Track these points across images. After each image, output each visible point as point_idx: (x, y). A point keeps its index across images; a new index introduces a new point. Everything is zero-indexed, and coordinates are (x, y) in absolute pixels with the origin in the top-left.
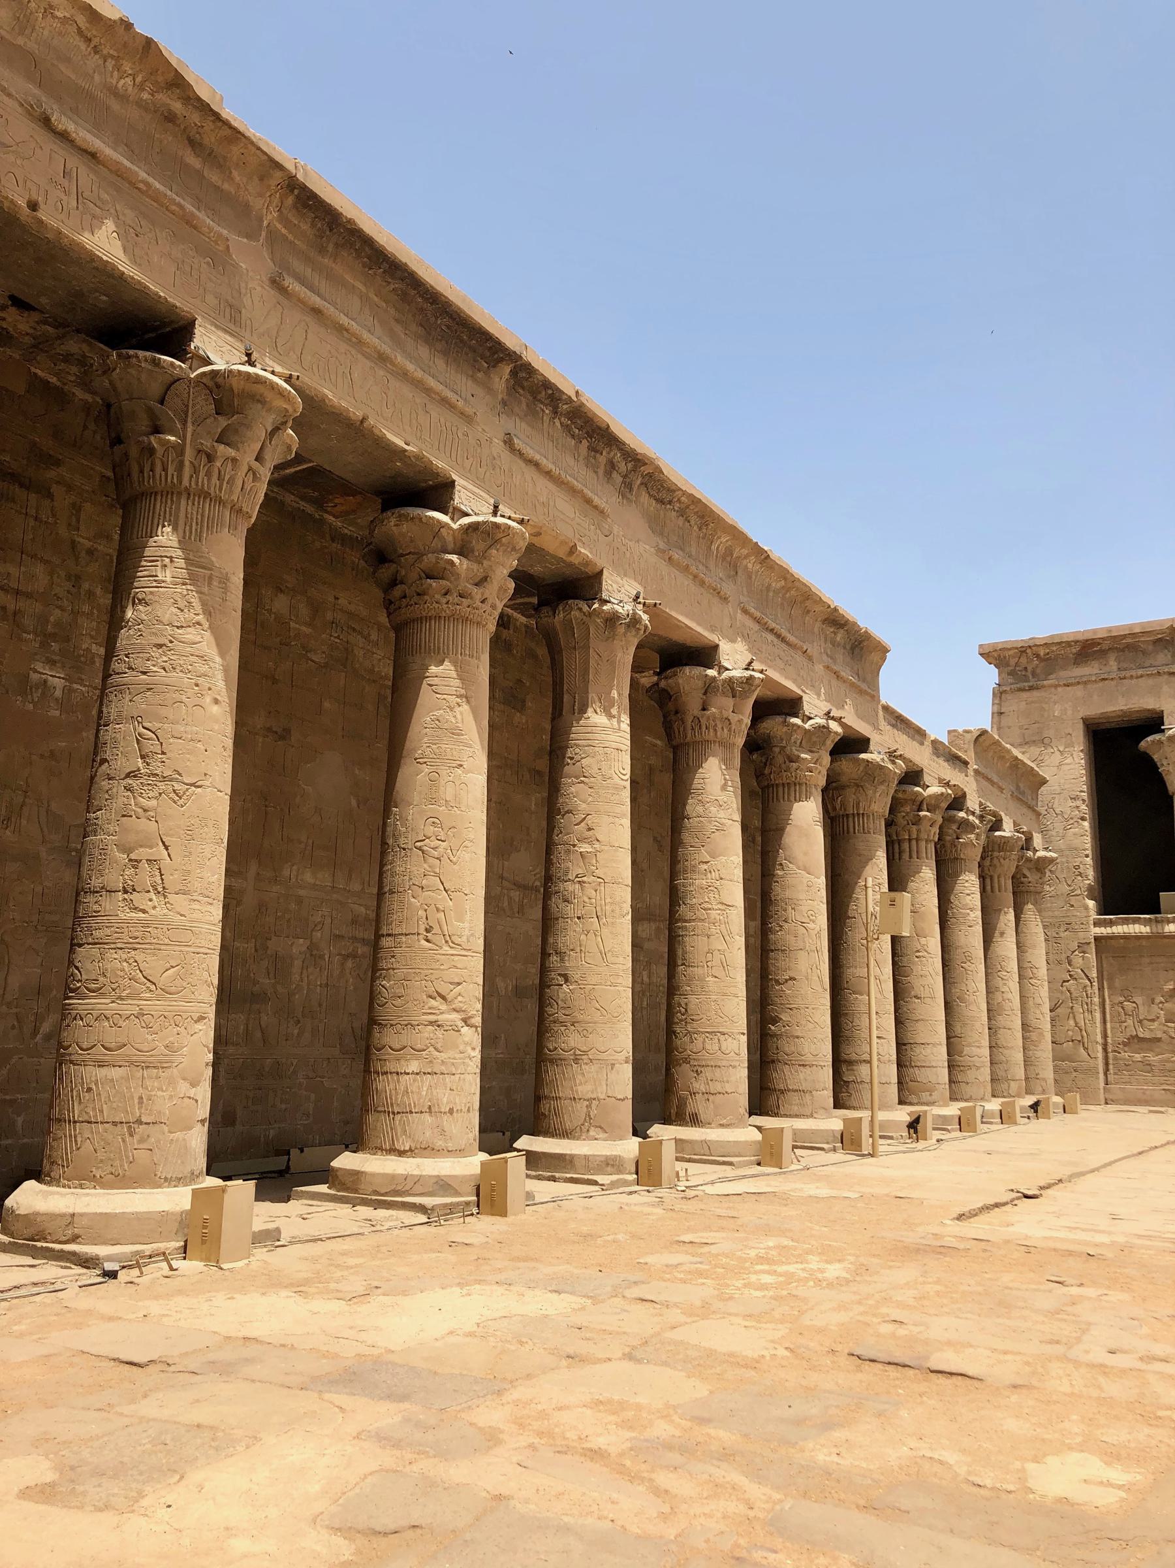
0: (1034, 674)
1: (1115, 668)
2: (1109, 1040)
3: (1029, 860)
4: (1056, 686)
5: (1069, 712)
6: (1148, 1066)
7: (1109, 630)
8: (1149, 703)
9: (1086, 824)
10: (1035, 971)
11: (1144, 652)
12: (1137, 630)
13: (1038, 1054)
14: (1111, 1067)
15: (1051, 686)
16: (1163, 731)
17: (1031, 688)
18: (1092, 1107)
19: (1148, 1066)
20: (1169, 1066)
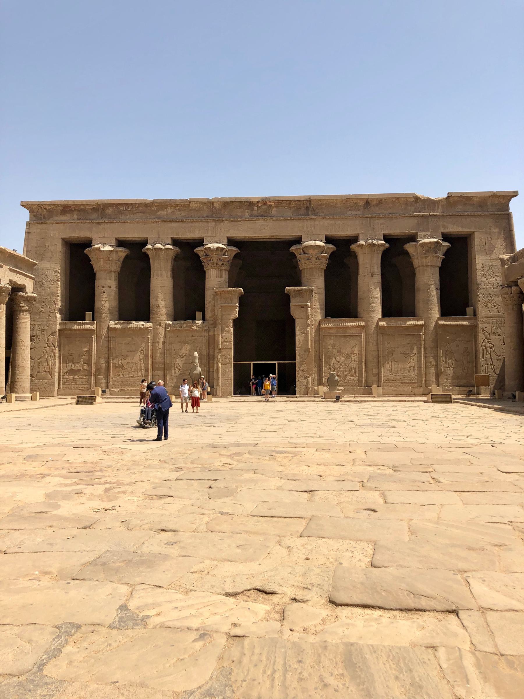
0: (44, 216)
1: (76, 218)
2: (62, 371)
3: (24, 297)
4: (52, 223)
5: (57, 235)
6: (75, 381)
7: (74, 202)
8: (87, 234)
9: (59, 283)
10: (23, 343)
11: (88, 213)
12: (84, 203)
13: (22, 377)
14: (61, 381)
15: (50, 223)
16: (92, 246)
17: (42, 223)
18: (51, 398)
19: (75, 381)
20: (83, 380)
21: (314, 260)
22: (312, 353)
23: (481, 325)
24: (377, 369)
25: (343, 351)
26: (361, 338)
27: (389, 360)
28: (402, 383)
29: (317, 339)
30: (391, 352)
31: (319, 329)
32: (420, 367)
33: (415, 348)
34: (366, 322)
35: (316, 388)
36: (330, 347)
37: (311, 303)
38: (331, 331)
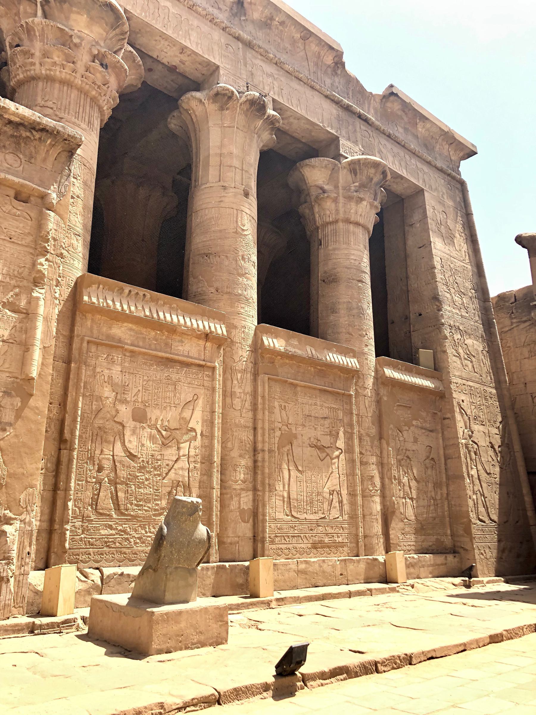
21: (83, 58)
22: (41, 404)
23: (457, 396)
24: (250, 493)
25: (153, 414)
26: (213, 379)
27: (285, 466)
28: (315, 546)
29: (62, 351)
30: (289, 439)
31: (74, 307)
32: (352, 495)
33: (341, 434)
34: (231, 327)
35: (37, 578)
36: (107, 392)
37: (61, 194)
38: (120, 331)
